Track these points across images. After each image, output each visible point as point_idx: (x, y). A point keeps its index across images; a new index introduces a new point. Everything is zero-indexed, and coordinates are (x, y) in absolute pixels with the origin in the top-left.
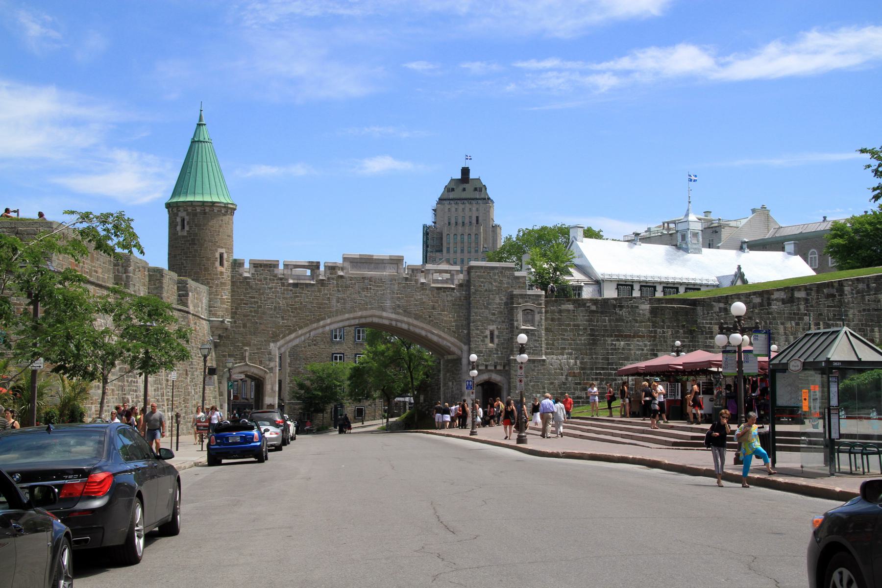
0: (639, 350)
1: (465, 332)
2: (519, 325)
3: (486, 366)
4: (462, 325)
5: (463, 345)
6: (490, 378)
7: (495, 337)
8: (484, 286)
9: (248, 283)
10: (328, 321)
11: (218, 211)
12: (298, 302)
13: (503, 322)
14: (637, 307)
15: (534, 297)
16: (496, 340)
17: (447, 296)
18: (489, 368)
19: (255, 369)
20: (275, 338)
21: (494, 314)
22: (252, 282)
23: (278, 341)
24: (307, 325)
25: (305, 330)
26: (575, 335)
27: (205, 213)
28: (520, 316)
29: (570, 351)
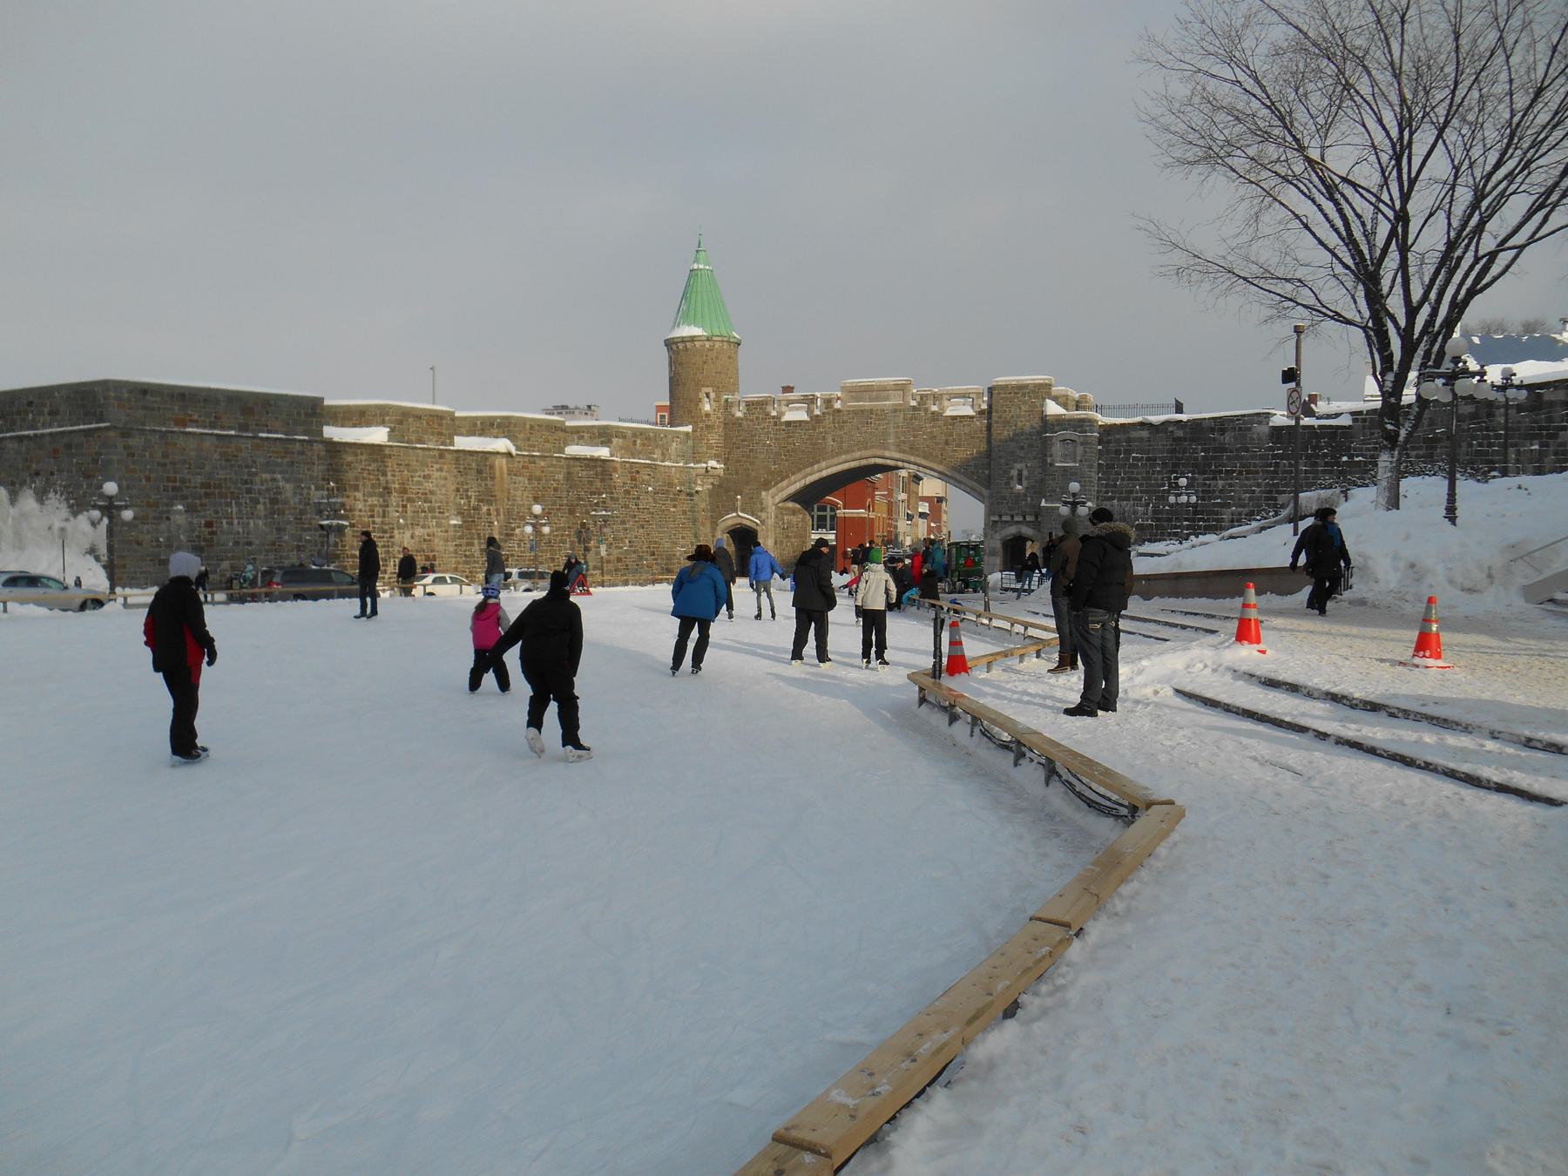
0: (1245, 492)
1: (987, 472)
2: (1053, 460)
3: (1012, 517)
4: (983, 464)
5: (984, 490)
6: (1020, 532)
7: (1023, 479)
8: (1010, 411)
9: (740, 425)
10: (824, 464)
11: (701, 346)
12: (791, 444)
13: (1035, 458)
14: (1249, 429)
15: (1076, 423)
16: (1025, 483)
17: (964, 426)
18: (1016, 519)
19: (748, 519)
20: (766, 486)
21: (1022, 448)
22: (745, 423)
23: (770, 488)
24: (800, 470)
25: (799, 476)
26: (1148, 473)
27: (686, 349)
28: (1057, 449)
29: (1139, 495)
